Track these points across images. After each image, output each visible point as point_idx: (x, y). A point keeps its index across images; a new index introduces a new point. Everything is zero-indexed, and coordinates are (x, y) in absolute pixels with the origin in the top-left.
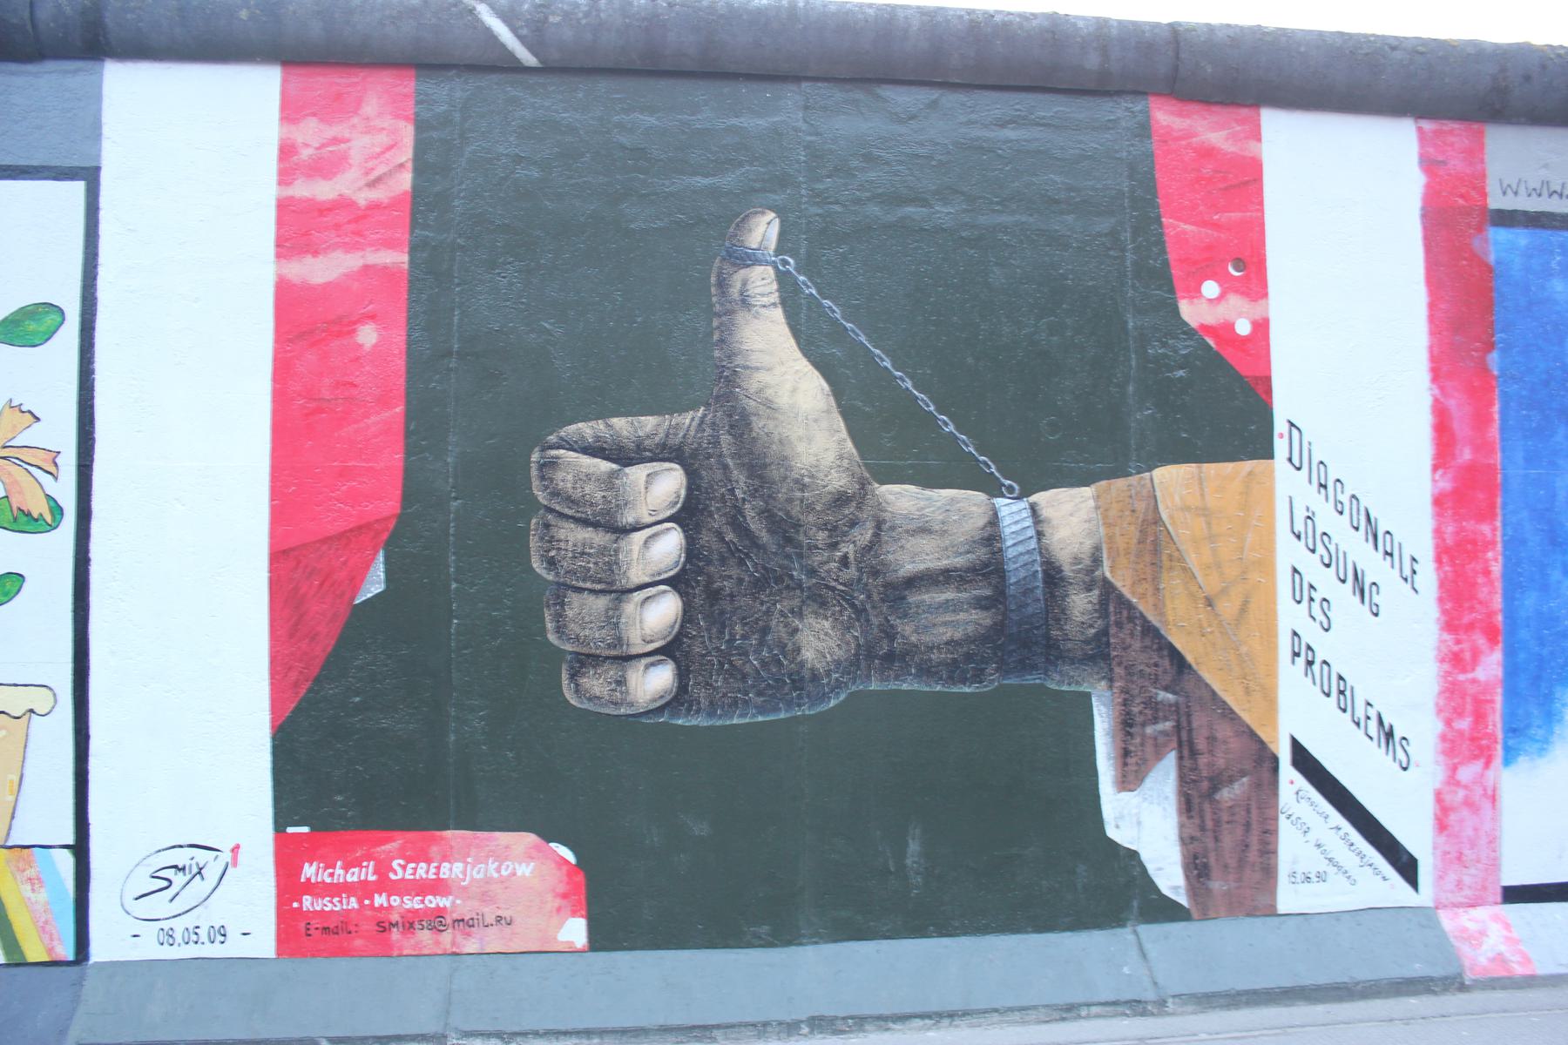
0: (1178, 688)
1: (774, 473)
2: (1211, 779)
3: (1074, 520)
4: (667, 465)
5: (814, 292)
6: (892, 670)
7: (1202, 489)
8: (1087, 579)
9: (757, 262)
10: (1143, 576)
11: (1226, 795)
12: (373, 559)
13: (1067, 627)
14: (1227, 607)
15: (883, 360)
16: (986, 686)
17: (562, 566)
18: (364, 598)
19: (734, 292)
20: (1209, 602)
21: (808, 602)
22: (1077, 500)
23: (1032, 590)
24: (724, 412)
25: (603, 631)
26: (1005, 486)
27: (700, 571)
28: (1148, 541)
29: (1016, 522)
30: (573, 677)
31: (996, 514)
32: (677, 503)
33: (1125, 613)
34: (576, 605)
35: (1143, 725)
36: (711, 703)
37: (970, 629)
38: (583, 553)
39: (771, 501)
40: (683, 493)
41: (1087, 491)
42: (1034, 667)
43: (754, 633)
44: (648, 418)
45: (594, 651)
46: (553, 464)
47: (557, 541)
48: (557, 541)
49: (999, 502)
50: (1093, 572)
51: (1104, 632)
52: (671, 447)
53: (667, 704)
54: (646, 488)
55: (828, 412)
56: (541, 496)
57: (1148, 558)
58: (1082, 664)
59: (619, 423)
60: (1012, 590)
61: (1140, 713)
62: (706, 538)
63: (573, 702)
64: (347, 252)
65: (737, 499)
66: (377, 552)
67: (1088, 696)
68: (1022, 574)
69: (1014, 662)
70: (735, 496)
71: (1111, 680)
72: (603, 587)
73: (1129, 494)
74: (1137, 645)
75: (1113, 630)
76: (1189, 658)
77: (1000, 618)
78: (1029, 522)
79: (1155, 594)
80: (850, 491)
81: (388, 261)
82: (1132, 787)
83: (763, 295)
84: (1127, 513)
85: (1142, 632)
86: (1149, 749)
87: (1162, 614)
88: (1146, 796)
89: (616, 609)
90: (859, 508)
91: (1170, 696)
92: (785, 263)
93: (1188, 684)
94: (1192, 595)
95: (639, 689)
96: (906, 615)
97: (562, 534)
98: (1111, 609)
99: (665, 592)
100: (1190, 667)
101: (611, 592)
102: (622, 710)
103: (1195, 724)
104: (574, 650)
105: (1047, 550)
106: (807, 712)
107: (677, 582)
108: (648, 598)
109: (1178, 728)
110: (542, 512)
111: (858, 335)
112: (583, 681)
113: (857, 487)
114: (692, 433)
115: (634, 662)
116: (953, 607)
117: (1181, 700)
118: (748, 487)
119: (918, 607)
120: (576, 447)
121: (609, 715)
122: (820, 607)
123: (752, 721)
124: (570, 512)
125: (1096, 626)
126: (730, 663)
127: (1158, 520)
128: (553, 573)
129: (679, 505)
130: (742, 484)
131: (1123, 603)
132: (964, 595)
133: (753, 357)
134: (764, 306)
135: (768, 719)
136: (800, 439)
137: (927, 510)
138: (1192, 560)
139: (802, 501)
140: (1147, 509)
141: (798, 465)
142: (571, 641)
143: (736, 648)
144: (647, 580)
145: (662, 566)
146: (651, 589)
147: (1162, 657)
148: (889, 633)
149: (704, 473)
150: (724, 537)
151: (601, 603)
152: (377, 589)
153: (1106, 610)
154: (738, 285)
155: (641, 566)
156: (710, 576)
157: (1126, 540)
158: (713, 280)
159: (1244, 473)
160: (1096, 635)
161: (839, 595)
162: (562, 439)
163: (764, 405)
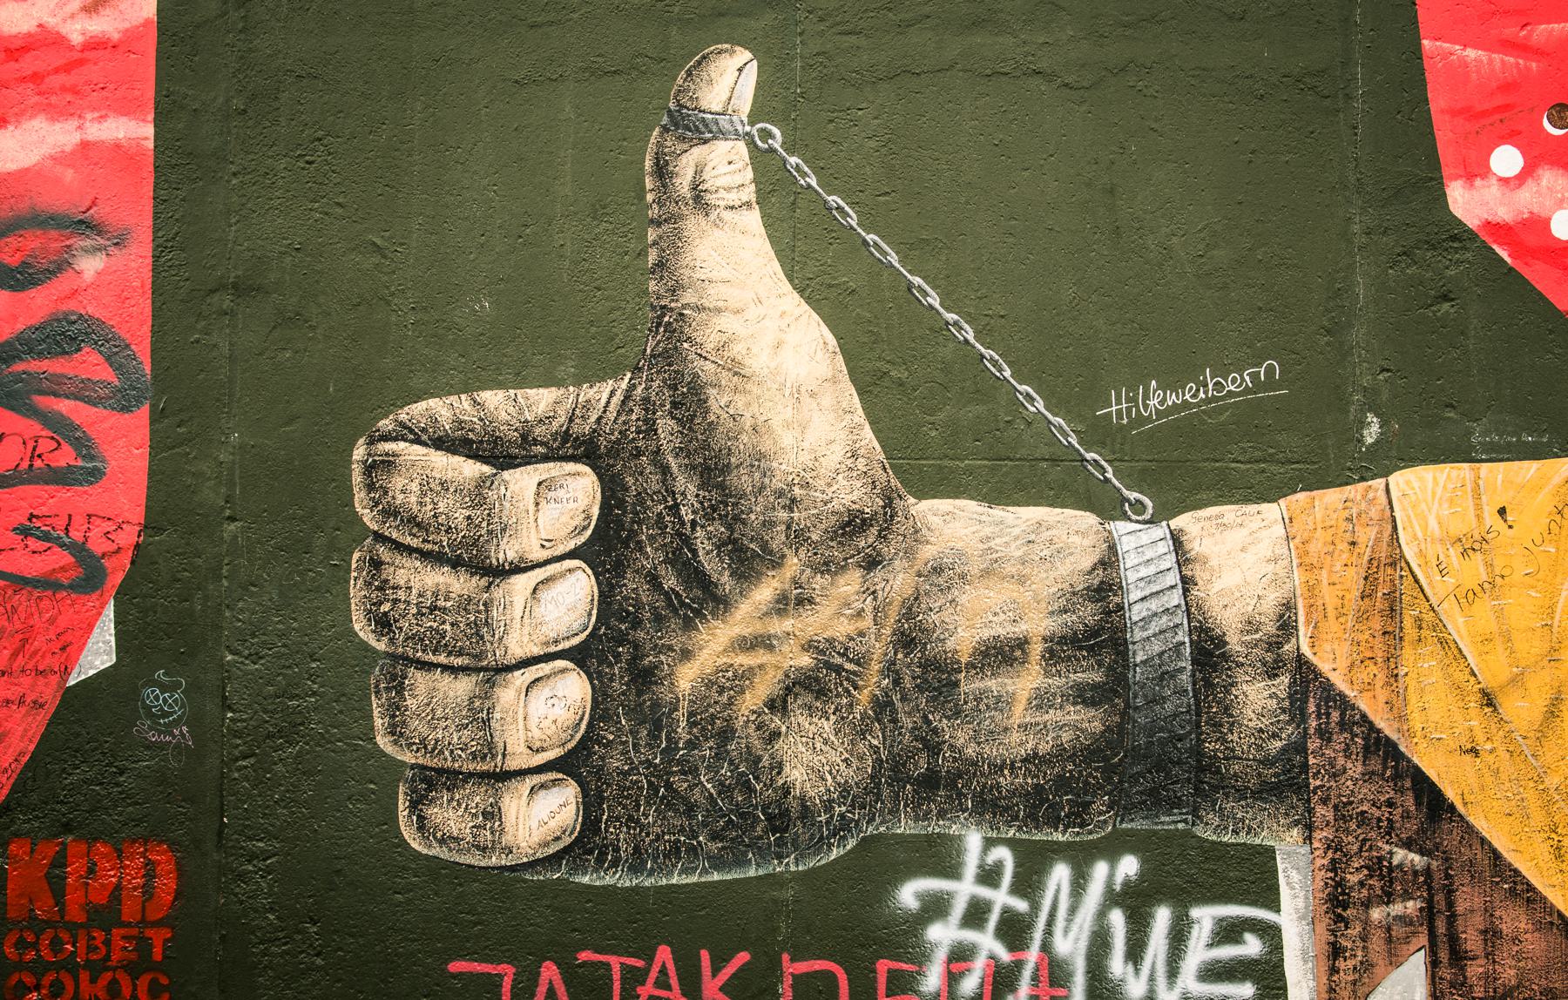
0: (1429, 844)
1: (743, 480)
4: (571, 467)
6: (934, 801)
8: (1269, 657)
9: (721, 134)
12: (100, 614)
15: (926, 294)
16: (1090, 833)
17: (401, 629)
18: (83, 677)
19: (683, 184)
21: (797, 689)
22: (1254, 526)
23: (1172, 675)
24: (664, 381)
25: (465, 732)
26: (1128, 500)
27: (621, 639)
28: (1380, 594)
30: (414, 806)
31: (1112, 548)
32: (585, 528)
33: (1335, 716)
35: (1367, 905)
36: (637, 849)
37: (1066, 736)
38: (433, 608)
39: (738, 526)
40: (596, 511)
41: (1271, 511)
42: (1175, 803)
43: (707, 740)
44: (541, 390)
45: (449, 764)
46: (388, 464)
47: (393, 588)
48: (393, 588)
49: (1120, 527)
50: (1279, 645)
51: (1300, 747)
52: (577, 438)
53: (566, 850)
54: (537, 504)
55: (834, 380)
56: (369, 518)
57: (1377, 624)
58: (1262, 799)
59: (493, 399)
60: (1139, 674)
61: (1362, 884)
62: (632, 584)
63: (415, 845)
64: (53, 120)
65: (683, 523)
66: (103, 606)
67: (1270, 853)
68: (1157, 647)
70: (680, 517)
71: (1309, 828)
72: (466, 662)
73: (1346, 514)
75: (1315, 743)
76: (1451, 794)
77: (1117, 719)
78: (1170, 561)
80: (867, 510)
81: (121, 135)
83: (728, 189)
84: (1344, 546)
85: (1366, 749)
86: (1377, 943)
87: (1402, 718)
90: (881, 536)
91: (1417, 858)
93: (1450, 838)
95: (521, 826)
96: (957, 713)
97: (401, 577)
98: (1312, 708)
99: (563, 671)
100: (1452, 808)
101: (478, 670)
102: (494, 859)
103: (1460, 908)
104: (420, 761)
105: (1199, 608)
106: (793, 868)
107: (580, 656)
108: (538, 680)
109: (1429, 913)
110: (369, 540)
111: (885, 254)
112: (435, 813)
113: (881, 503)
114: (611, 415)
115: (514, 783)
117: (1435, 864)
118: (702, 503)
119: (978, 700)
120: (424, 438)
121: (473, 867)
122: (817, 698)
123: (703, 880)
124: (414, 543)
125: (1284, 736)
126: (668, 786)
127: (1396, 560)
128: (385, 639)
129: (589, 532)
130: (693, 500)
131: (1332, 698)
132: (1057, 682)
133: (712, 290)
134: (732, 208)
135: (729, 877)
136: (787, 425)
137: (998, 541)
138: (1457, 625)
139: (789, 527)
140: (1378, 540)
141: (783, 467)
142: (415, 747)
143: (679, 762)
144: (537, 651)
145: (563, 631)
146: (543, 665)
147: (1401, 791)
148: (931, 744)
149: (630, 480)
150: (661, 583)
151: (463, 687)
152: (102, 664)
154: (690, 173)
155: (526, 630)
156: (636, 647)
158: (648, 164)
160: (1284, 750)
161: (847, 679)
162: (402, 425)
163: (730, 370)
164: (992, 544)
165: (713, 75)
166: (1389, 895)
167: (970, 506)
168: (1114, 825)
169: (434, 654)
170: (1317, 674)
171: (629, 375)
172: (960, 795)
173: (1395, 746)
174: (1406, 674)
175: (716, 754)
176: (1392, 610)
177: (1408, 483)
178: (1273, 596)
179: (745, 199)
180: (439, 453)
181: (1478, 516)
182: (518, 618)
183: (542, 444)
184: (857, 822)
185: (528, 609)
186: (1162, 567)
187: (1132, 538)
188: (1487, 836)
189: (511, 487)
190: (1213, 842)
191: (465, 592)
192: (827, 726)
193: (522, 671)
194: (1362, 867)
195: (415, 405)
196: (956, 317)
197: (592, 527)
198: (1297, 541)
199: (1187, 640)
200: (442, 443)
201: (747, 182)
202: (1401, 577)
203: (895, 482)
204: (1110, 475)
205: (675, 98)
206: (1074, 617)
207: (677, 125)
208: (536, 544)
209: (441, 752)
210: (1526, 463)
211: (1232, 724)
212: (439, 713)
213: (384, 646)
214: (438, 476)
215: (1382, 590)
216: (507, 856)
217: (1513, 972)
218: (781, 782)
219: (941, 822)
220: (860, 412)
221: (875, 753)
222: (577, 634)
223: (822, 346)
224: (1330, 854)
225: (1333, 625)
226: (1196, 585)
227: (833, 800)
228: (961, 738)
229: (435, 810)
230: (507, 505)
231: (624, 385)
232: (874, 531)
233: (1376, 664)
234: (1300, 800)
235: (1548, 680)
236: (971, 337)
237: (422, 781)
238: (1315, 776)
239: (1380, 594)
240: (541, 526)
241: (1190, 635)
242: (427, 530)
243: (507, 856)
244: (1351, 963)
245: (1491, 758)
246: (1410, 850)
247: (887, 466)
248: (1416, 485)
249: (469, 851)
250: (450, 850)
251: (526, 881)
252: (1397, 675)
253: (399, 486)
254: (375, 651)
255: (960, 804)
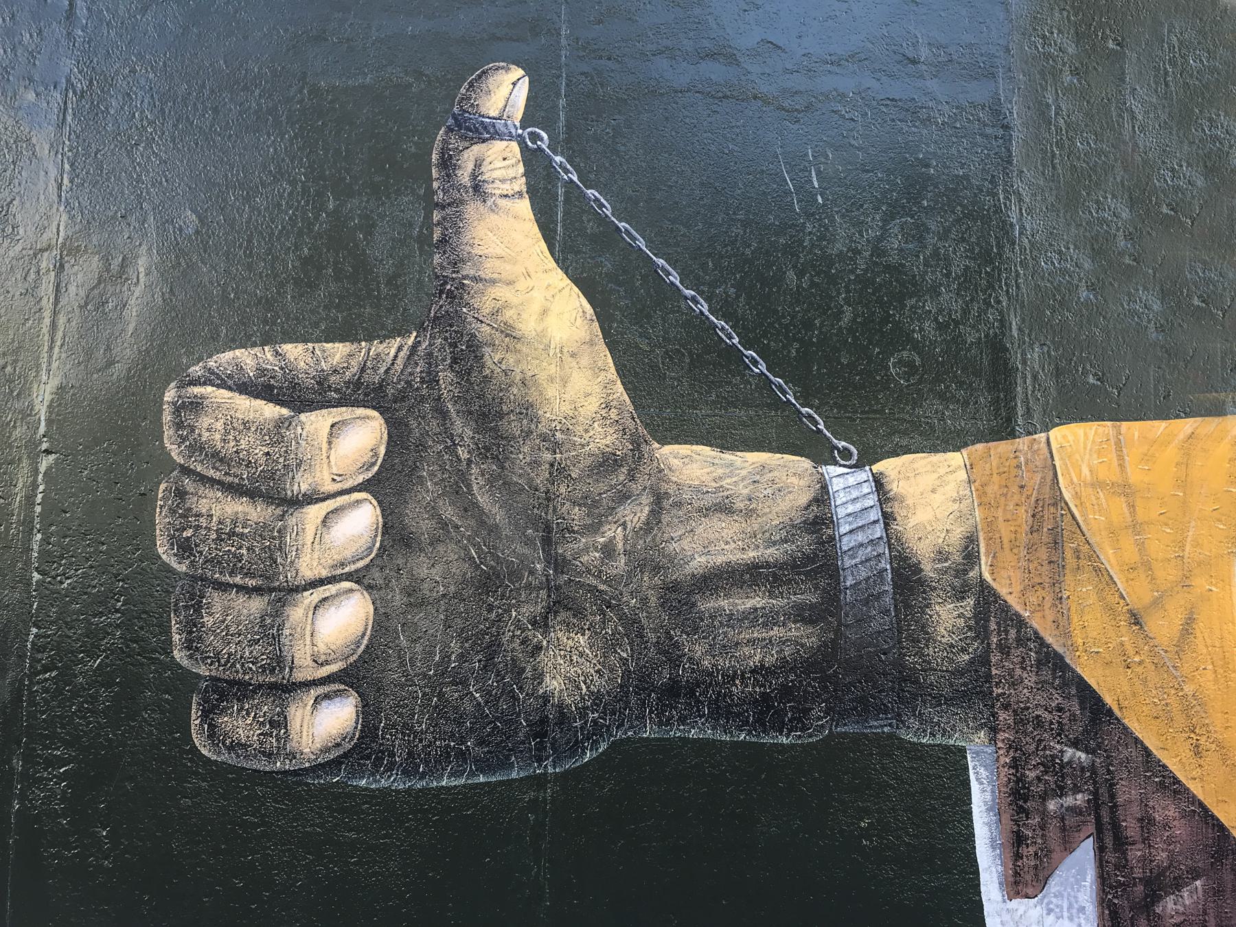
1: (513, 427)
2: (1147, 882)
3: (938, 498)
4: (361, 411)
5: (575, 178)
6: (675, 708)
7: (1121, 458)
8: (957, 583)
9: (496, 135)
10: (1038, 580)
11: (1169, 905)
13: (931, 651)
14: (1164, 628)
15: (669, 274)
16: (810, 736)
17: (201, 553)
19: (464, 176)
20: (1136, 619)
22: (942, 471)
23: (878, 597)
25: (257, 647)
28: (1045, 530)
29: (855, 500)
30: (206, 715)
31: (824, 488)
32: (373, 464)
33: (1013, 633)
34: (217, 608)
35: (1044, 798)
36: (410, 754)
37: (788, 651)
38: (232, 534)
40: (382, 450)
41: (956, 459)
42: (884, 710)
44: (337, 345)
46: (196, 405)
48: (196, 516)
49: (832, 470)
50: (965, 572)
51: (983, 660)
53: (346, 755)
55: (591, 343)
56: (176, 453)
57: (1043, 554)
58: (953, 705)
59: (294, 351)
61: (1038, 778)
63: (204, 752)
67: (962, 752)
68: (864, 573)
69: (852, 700)
70: (457, 457)
71: (994, 730)
74: (1030, 679)
75: (995, 658)
76: (1109, 700)
78: (872, 500)
79: (1055, 605)
80: (618, 453)
82: (1030, 891)
83: (503, 181)
84: (1015, 489)
85: (1039, 662)
87: (1067, 635)
88: (1051, 906)
89: (277, 614)
91: (1083, 756)
92: (535, 137)
94: (1110, 609)
95: (305, 733)
96: (696, 630)
97: (203, 506)
98: (993, 626)
99: (351, 591)
100: (1110, 712)
101: (271, 590)
102: (278, 764)
103: (1120, 800)
105: (898, 540)
106: (550, 770)
108: (325, 599)
109: (1095, 804)
111: (634, 239)
113: (631, 447)
116: (769, 619)
118: (477, 444)
120: (230, 383)
121: (259, 771)
124: (217, 475)
125: (971, 650)
126: (441, 695)
127: (1058, 500)
129: (376, 468)
133: (488, 264)
134: (506, 196)
136: (551, 379)
137: (728, 481)
138: (1109, 557)
139: (552, 465)
141: (548, 415)
142: (209, 661)
144: (325, 573)
145: (348, 554)
148: (672, 654)
151: (256, 605)
153: (986, 628)
154: (470, 166)
155: (316, 555)
157: (1012, 529)
158: (435, 157)
159: (1181, 436)
160: (971, 662)
164: (723, 483)
165: (491, 87)
166: (1062, 788)
167: (706, 450)
168: (831, 729)
169: (231, 576)
170: (997, 596)
171: (415, 334)
172: (698, 701)
173: (1061, 658)
174: (1068, 597)
175: (485, 667)
176: (1056, 543)
177: (1064, 437)
178: (959, 531)
179: (517, 189)
180: (243, 397)
181: (1120, 465)
182: (309, 543)
183: (336, 391)
184: (608, 730)
185: (318, 536)
186: (867, 505)
187: (841, 480)
188: (1140, 736)
189: (307, 427)
190: (914, 743)
191: (261, 519)
192: (582, 640)
193: (311, 591)
194: (1038, 764)
195: (223, 354)
196: (693, 293)
197: (379, 463)
198: (976, 484)
199: (888, 567)
200: (245, 388)
201: (519, 175)
202: (1062, 515)
203: (642, 430)
204: (821, 427)
205: (459, 103)
206: (794, 547)
207: (460, 127)
208: (327, 478)
209: (233, 665)
210: (1156, 423)
211: (928, 641)
212: (232, 630)
213: (185, 568)
214: (241, 417)
215: (1048, 525)
216: (291, 761)
217: (1164, 855)
218: (541, 691)
219: (682, 727)
220: (613, 370)
221: (624, 665)
222: (362, 559)
223: (581, 314)
224: (1012, 754)
225: (1007, 557)
226: (895, 520)
227: (588, 707)
228: (699, 650)
229: (226, 719)
230: (303, 443)
231: (410, 341)
232: (624, 470)
233: (1044, 589)
234: (985, 705)
235: (1182, 602)
236: (706, 310)
237: (214, 692)
238: (997, 684)
239: (1045, 530)
240: (333, 463)
241: (891, 563)
242: (229, 465)
243: (291, 761)
244: (1032, 850)
245: (1139, 669)
246: (1078, 749)
247: (635, 416)
248: (1071, 438)
249: (255, 756)
250: (238, 756)
251: (307, 784)
252: (1061, 598)
253: (205, 425)
254: (178, 573)
255: (698, 710)
